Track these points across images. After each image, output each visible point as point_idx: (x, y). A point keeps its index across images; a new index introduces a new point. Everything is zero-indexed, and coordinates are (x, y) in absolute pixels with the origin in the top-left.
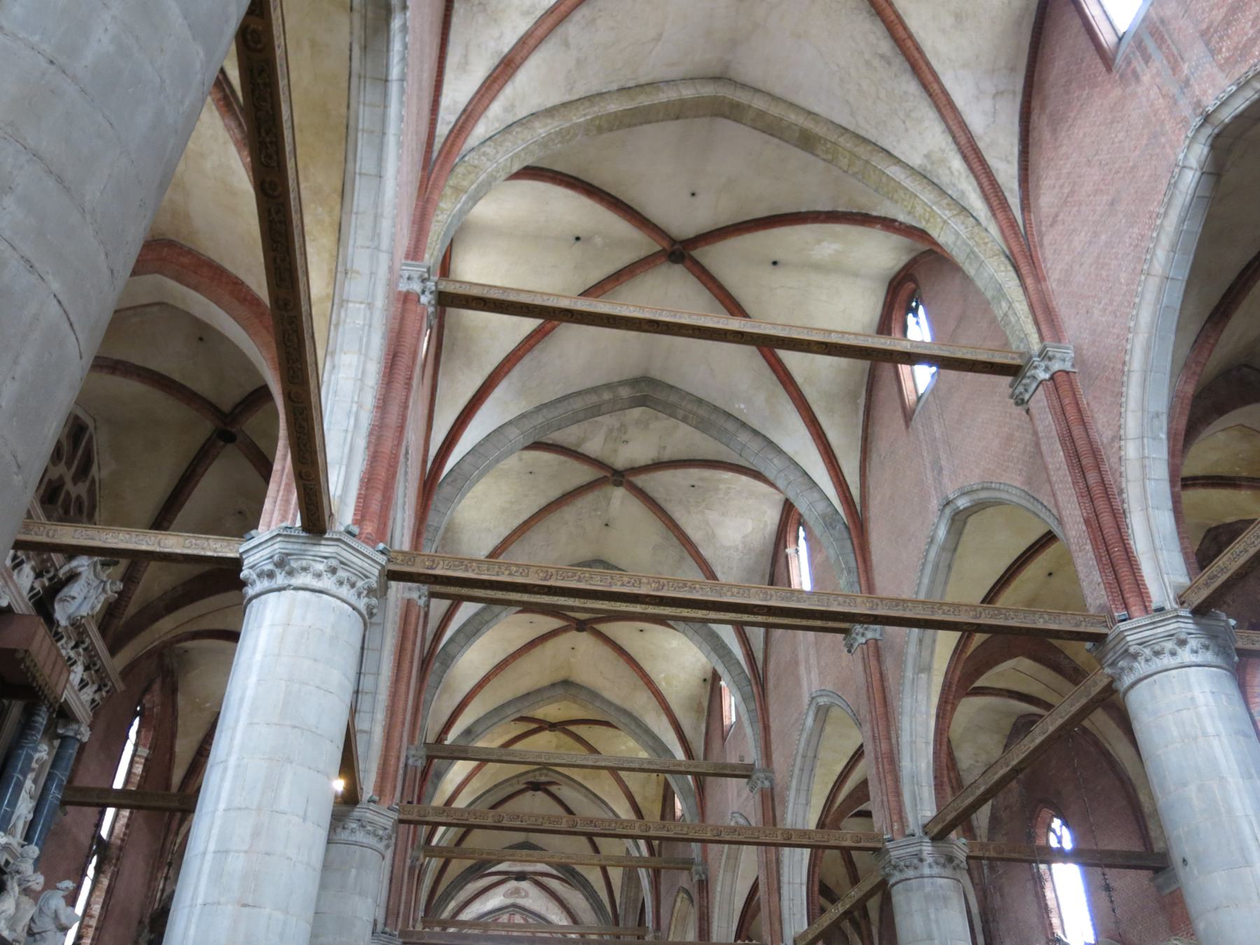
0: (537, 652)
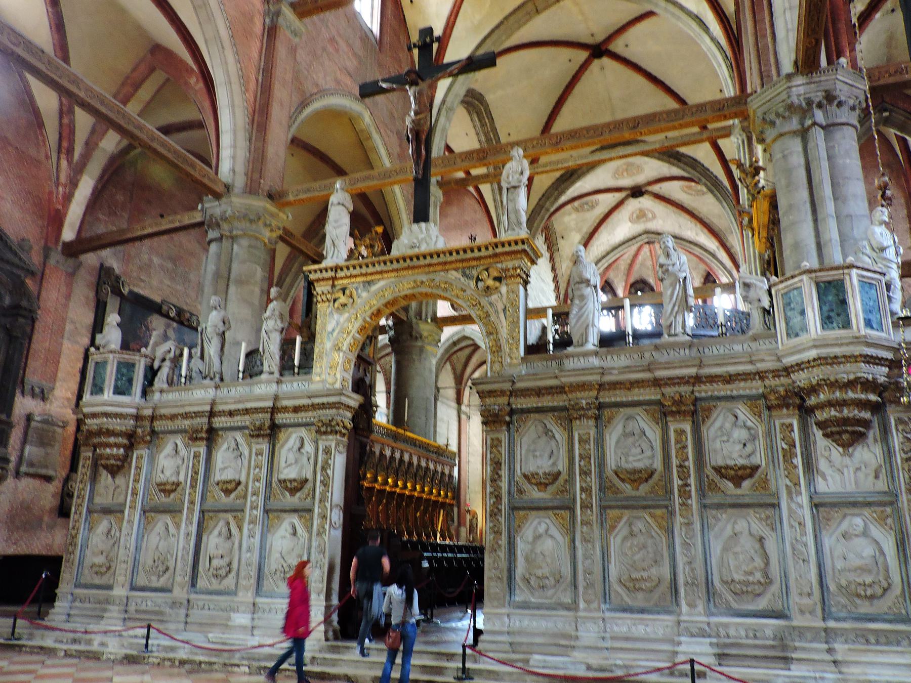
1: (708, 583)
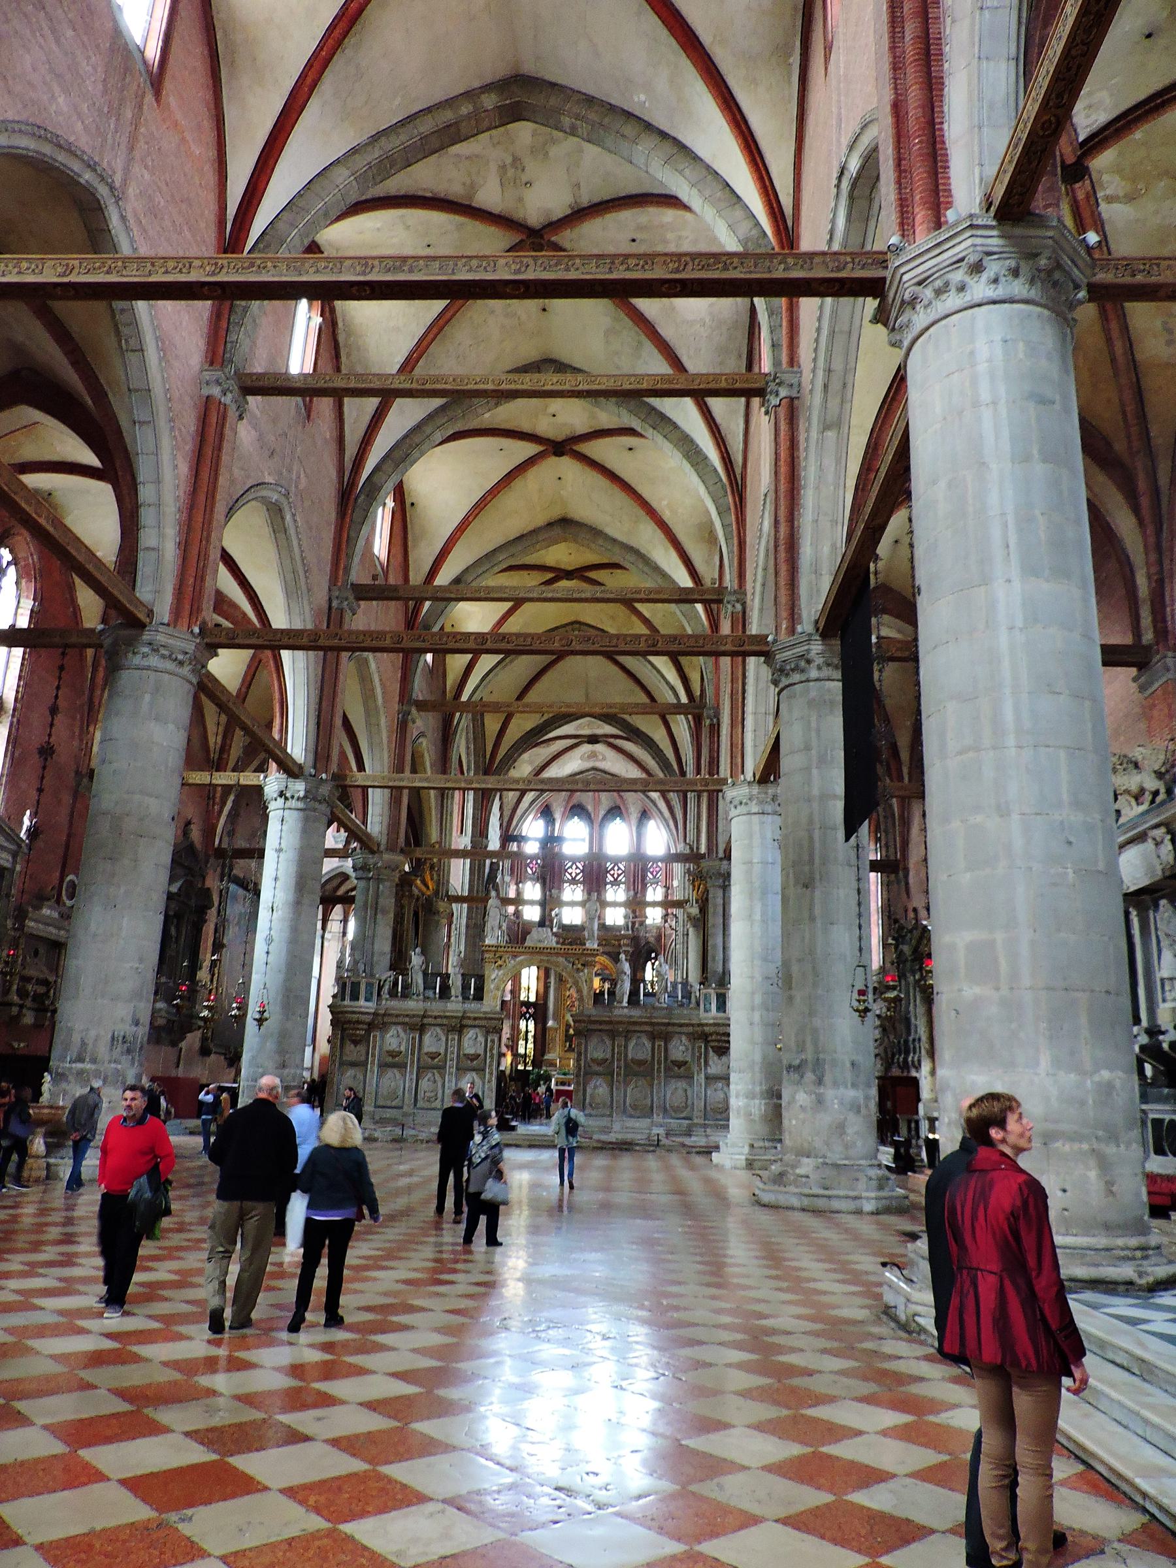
0: (518, 484)
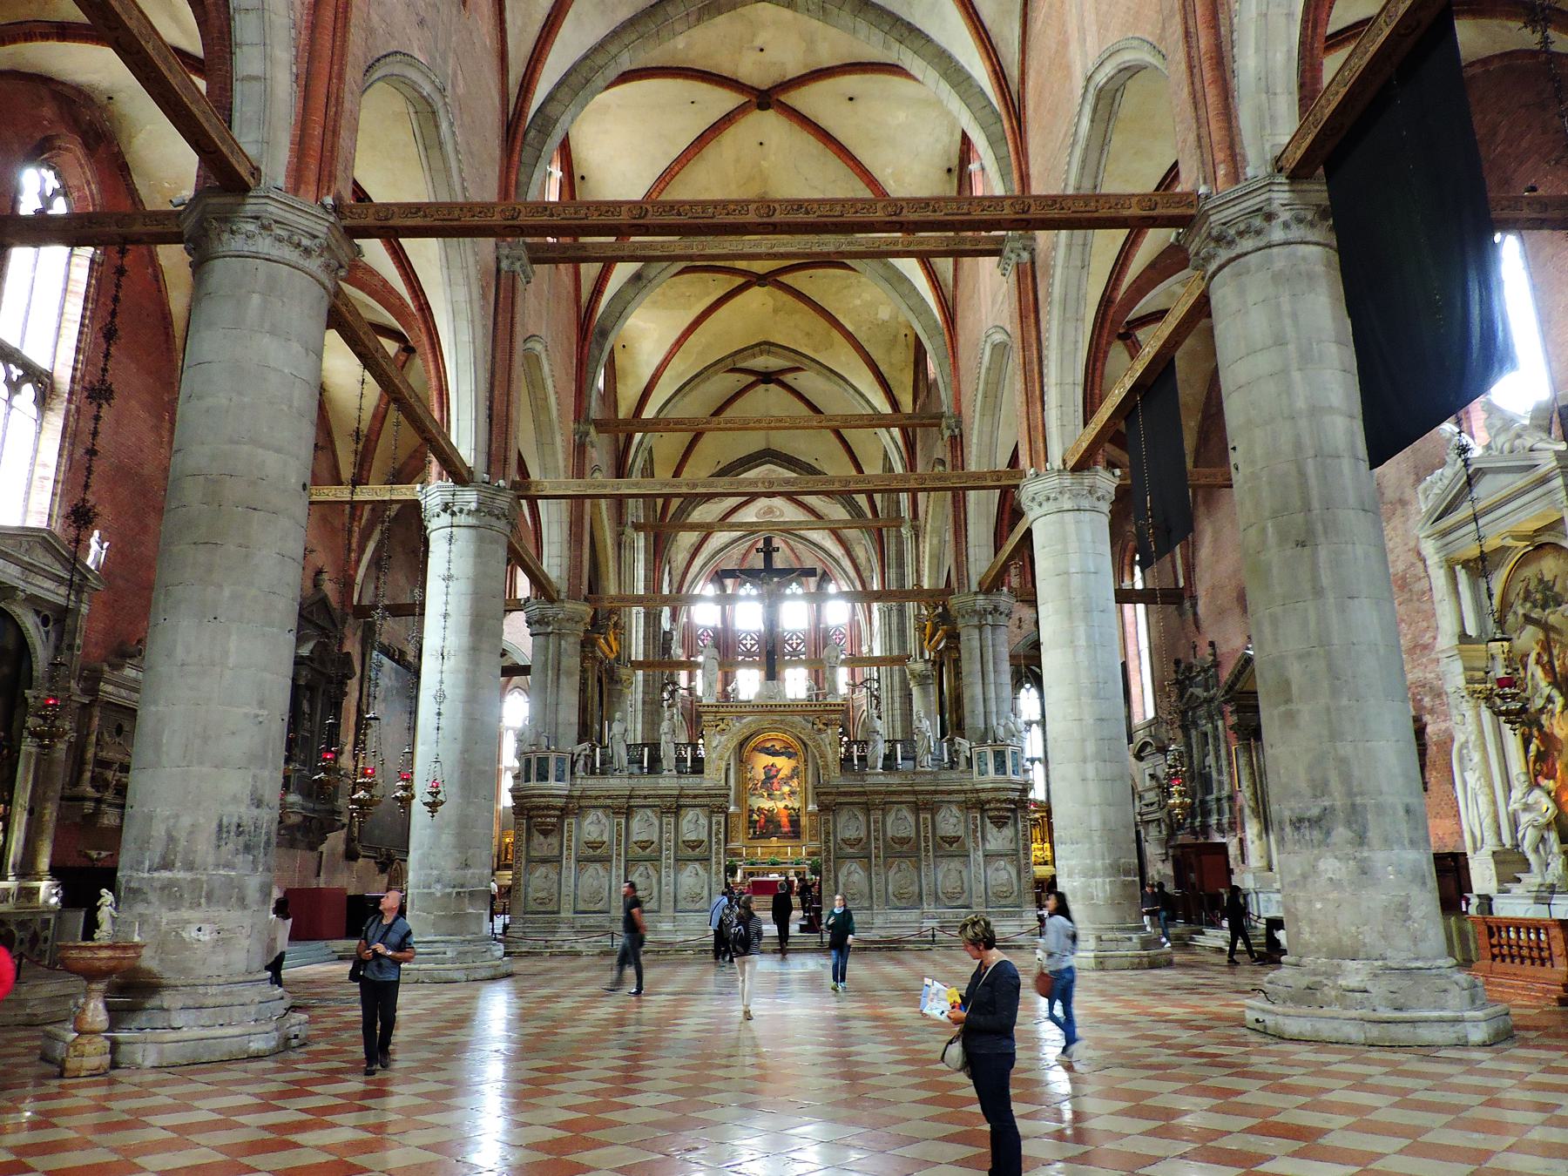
0: (711, 151)
1: (936, 893)
